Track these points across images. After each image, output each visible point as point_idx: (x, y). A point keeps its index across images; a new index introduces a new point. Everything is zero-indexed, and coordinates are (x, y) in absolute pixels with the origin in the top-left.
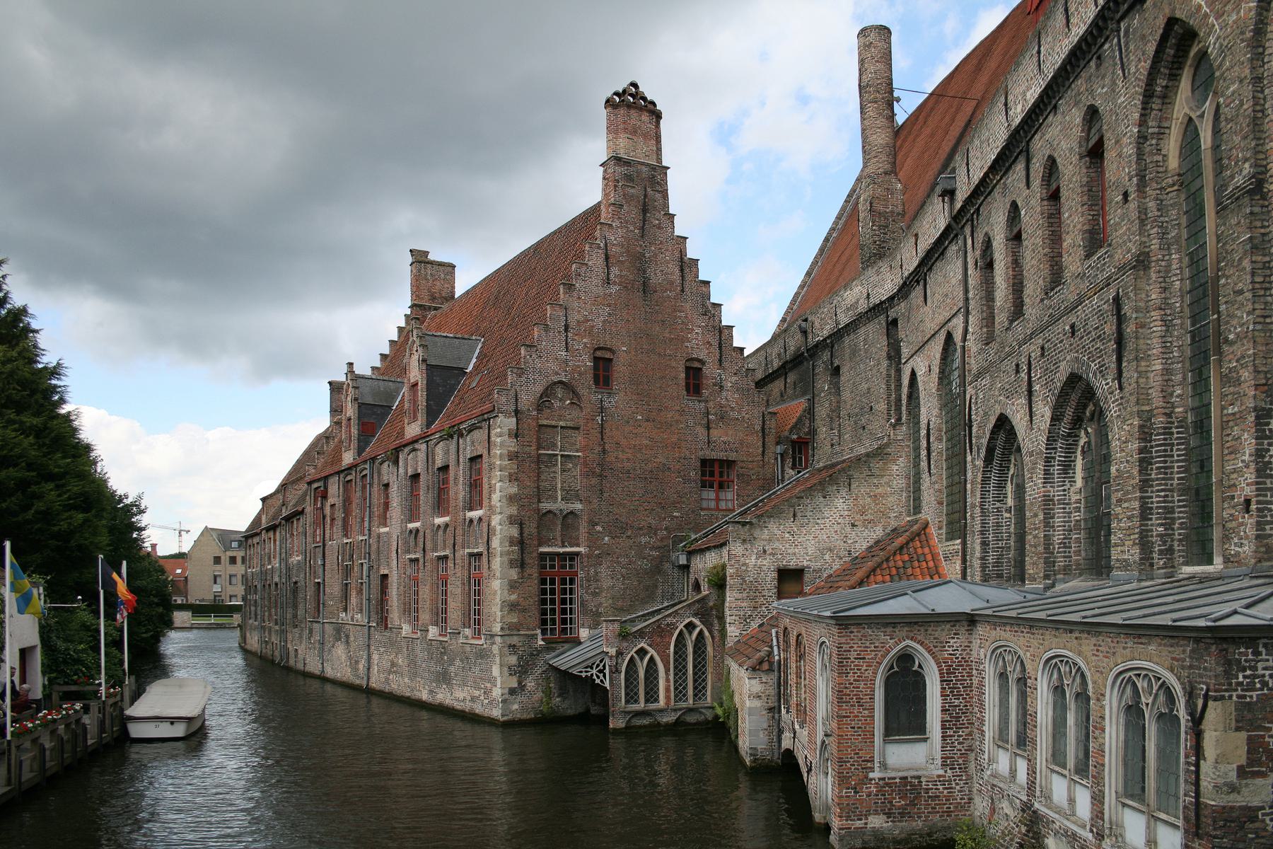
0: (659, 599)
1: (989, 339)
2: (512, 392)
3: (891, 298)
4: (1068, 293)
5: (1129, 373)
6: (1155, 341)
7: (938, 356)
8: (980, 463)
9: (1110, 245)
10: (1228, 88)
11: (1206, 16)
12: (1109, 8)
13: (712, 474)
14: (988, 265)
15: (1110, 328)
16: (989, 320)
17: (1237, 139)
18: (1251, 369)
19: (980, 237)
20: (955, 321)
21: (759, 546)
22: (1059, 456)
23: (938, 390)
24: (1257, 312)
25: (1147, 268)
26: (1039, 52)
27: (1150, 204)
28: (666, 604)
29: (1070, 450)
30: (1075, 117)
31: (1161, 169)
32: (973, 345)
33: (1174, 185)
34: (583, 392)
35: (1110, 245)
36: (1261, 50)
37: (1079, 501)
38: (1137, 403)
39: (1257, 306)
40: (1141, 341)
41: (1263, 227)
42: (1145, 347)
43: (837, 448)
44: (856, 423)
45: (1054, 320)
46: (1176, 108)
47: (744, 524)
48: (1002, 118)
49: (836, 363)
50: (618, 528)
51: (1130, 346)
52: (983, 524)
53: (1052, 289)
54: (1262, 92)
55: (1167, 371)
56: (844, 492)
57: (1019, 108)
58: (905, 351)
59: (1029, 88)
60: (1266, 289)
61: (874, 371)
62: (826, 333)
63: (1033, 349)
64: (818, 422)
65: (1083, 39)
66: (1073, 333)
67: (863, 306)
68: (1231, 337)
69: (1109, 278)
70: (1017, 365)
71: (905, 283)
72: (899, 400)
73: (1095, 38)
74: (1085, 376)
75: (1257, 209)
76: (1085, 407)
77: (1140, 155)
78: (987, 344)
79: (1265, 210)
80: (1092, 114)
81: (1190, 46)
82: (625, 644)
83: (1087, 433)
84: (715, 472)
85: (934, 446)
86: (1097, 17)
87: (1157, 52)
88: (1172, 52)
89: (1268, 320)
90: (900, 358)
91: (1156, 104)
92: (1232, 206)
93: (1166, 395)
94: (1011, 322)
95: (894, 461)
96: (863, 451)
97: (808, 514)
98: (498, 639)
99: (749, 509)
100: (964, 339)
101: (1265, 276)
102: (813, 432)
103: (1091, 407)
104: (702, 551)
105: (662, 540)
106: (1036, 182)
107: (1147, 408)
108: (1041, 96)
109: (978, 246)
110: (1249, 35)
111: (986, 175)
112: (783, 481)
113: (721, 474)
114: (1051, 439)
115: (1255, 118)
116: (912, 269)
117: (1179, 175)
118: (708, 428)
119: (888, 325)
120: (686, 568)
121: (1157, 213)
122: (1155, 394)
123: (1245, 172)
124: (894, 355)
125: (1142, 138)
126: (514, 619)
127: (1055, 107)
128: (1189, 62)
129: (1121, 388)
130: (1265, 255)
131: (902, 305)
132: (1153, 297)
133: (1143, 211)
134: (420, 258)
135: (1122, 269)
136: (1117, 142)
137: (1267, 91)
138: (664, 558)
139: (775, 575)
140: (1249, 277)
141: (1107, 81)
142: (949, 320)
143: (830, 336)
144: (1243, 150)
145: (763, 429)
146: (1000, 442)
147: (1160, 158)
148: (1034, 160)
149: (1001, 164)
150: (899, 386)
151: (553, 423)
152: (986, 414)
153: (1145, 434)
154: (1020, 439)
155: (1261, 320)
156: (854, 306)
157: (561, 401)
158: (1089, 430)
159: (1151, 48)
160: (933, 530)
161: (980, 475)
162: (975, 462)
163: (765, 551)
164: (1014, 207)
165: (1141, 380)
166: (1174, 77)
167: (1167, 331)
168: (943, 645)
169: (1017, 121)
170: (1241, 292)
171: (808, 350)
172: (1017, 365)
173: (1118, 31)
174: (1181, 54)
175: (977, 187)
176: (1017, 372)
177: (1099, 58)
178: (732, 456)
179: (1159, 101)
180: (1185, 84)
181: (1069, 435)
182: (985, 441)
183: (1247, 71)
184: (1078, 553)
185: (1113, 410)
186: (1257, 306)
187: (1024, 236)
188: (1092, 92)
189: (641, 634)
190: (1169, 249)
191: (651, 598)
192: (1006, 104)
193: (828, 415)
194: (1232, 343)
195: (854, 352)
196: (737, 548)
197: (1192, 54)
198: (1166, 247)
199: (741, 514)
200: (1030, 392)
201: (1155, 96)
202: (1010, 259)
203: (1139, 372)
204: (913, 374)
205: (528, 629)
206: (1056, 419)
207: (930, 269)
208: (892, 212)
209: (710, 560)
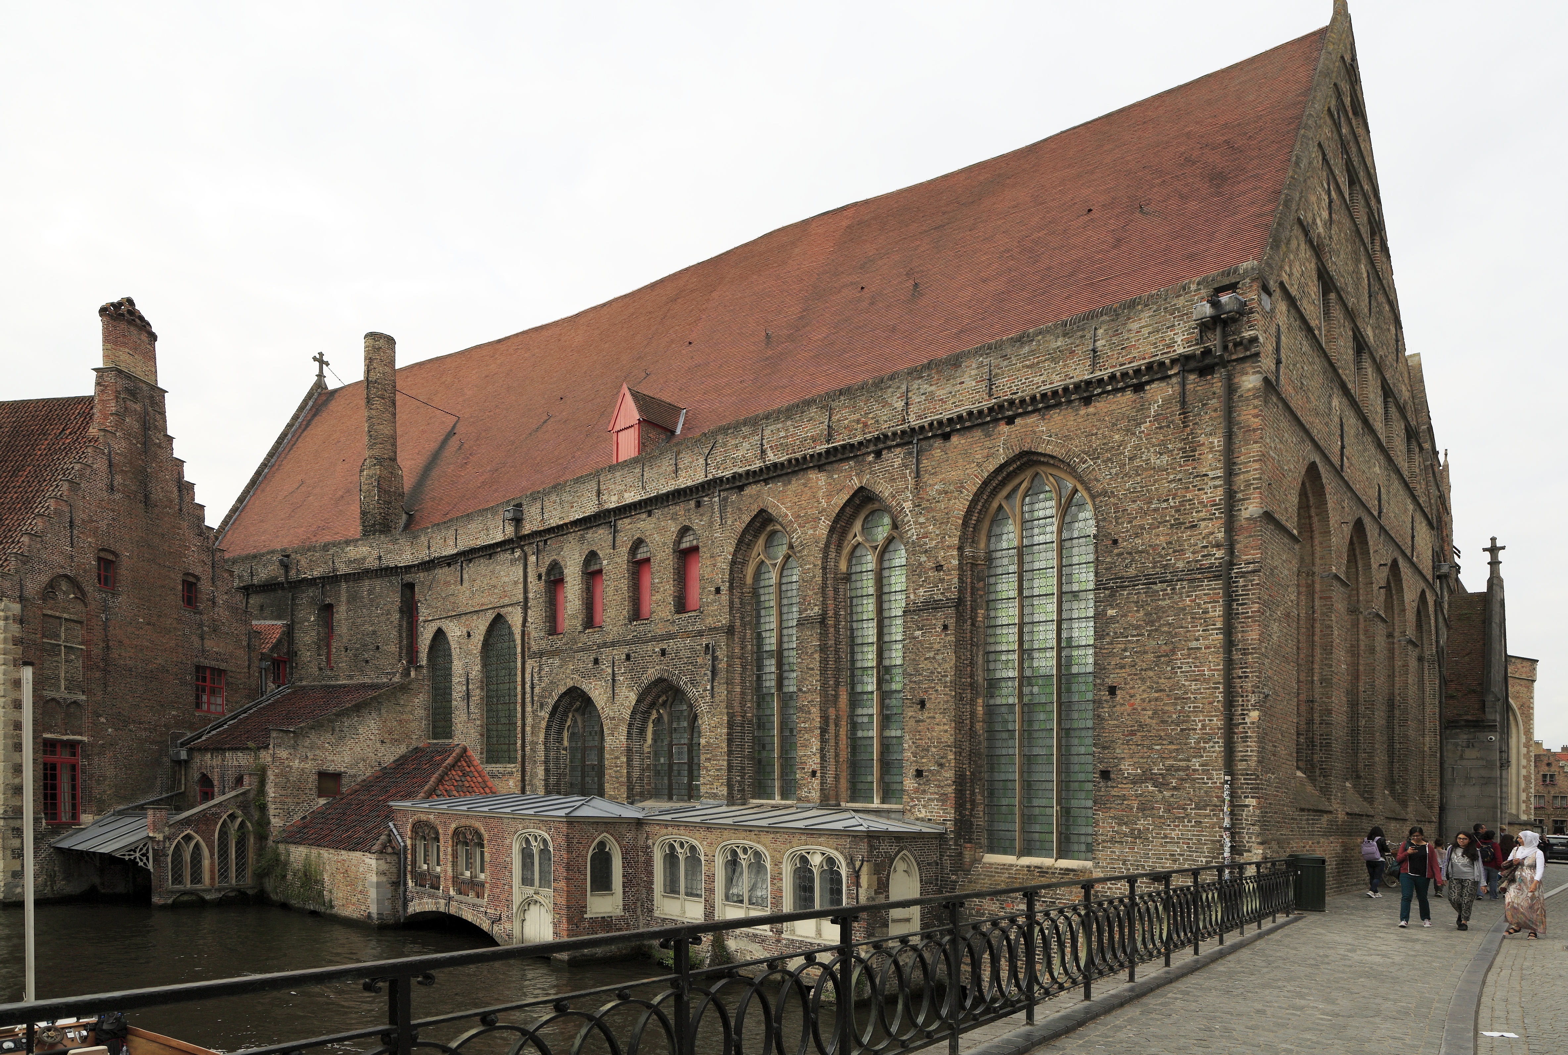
2: (17, 578)
13: (204, 679)
34: (89, 589)
37: (649, 753)
52: (546, 756)
84: (207, 678)
118: (202, 639)
151: (57, 614)
157: (65, 594)
160: (476, 757)
184: (649, 784)
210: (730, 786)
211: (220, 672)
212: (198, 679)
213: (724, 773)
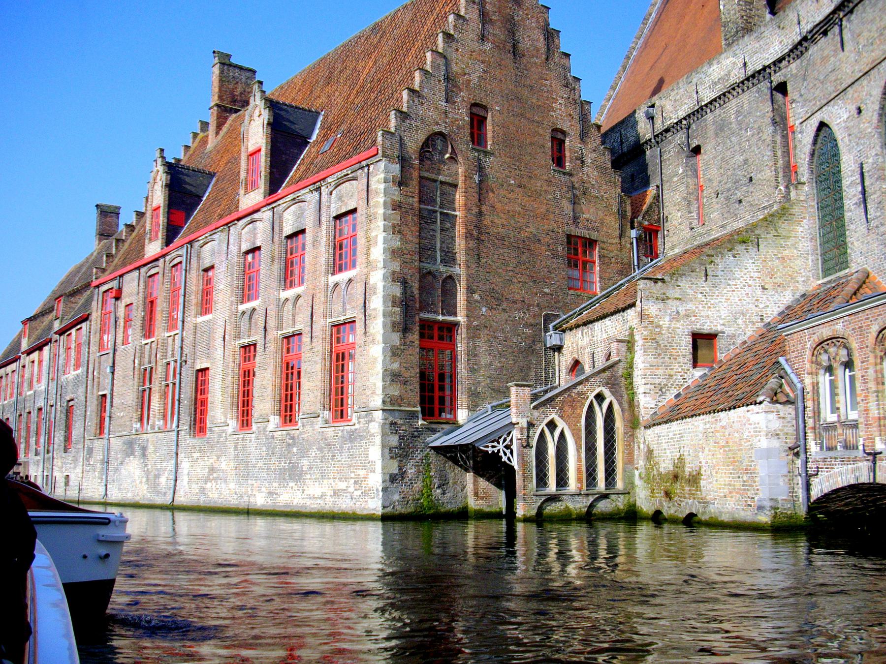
3: (780, 60)
23: (877, 127)
44: (727, 199)
49: (694, 143)
50: (495, 299)
62: (682, 114)
67: (737, 75)
82: (536, 413)
95: (799, 223)
96: (741, 224)
97: (720, 273)
98: (379, 415)
99: (611, 292)
119: (772, 90)
124: (780, 121)
126: (395, 391)
134: (225, 62)
138: (536, 338)
139: (689, 339)
143: (689, 116)
163: (678, 312)
171: (655, 136)
178: (594, 236)
193: (685, 199)
195: (721, 127)
196: (652, 309)
205: (409, 405)
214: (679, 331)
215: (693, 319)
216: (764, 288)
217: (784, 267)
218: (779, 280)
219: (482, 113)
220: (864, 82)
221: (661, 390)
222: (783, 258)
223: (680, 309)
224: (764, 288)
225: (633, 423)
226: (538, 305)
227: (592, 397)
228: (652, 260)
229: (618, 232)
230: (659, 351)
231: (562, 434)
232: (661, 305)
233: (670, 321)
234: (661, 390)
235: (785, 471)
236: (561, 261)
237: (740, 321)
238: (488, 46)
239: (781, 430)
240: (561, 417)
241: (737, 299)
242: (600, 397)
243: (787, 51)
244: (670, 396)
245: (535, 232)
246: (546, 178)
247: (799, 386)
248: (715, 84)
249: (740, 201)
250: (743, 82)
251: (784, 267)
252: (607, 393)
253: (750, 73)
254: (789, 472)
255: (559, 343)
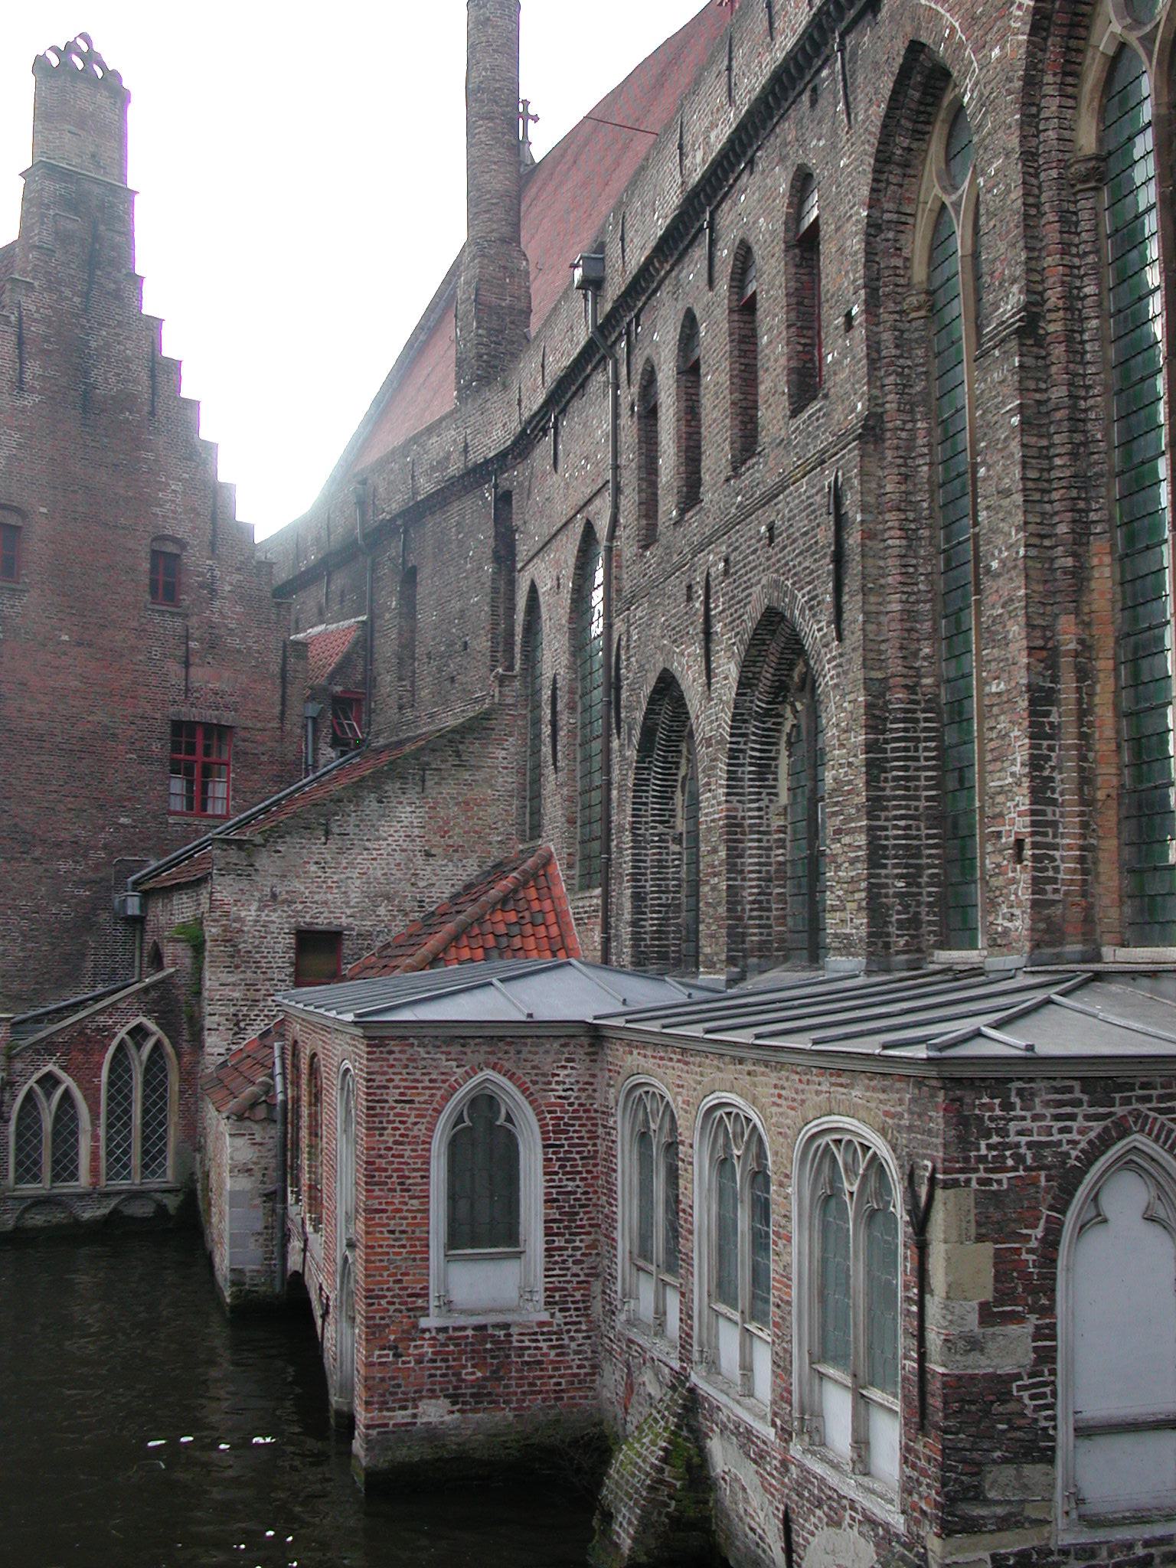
0: (87, 980)
1: (649, 538)
3: (502, 456)
4: (763, 472)
5: (854, 613)
6: (890, 562)
7: (572, 561)
8: (632, 754)
9: (826, 396)
10: (990, 164)
11: (961, 43)
12: (828, 13)
13: (191, 750)
14: (649, 414)
15: (825, 535)
16: (649, 506)
17: (1002, 246)
18: (1022, 620)
19: (639, 365)
20: (597, 502)
21: (266, 882)
22: (752, 749)
23: (571, 620)
24: (1031, 528)
25: (879, 440)
26: (729, 69)
27: (885, 336)
28: (100, 989)
29: (768, 739)
30: (782, 183)
31: (902, 281)
32: (627, 547)
33: (918, 309)
35: (826, 396)
36: (1034, 110)
38: (864, 666)
39: (1031, 518)
40: (870, 562)
41: (1037, 390)
42: (875, 572)
43: (409, 714)
44: (440, 671)
45: (746, 514)
46: (924, 187)
47: (240, 844)
48: (672, 165)
49: (412, 560)
51: (854, 567)
53: (743, 462)
54: (1036, 176)
55: (909, 615)
56: (412, 794)
57: (699, 155)
58: (523, 550)
59: (713, 125)
60: (1044, 491)
61: (472, 581)
63: (713, 561)
64: (380, 666)
65: (791, 57)
66: (771, 539)
68: (995, 564)
69: (824, 451)
70: (689, 587)
71: (524, 430)
72: (510, 634)
73: (809, 60)
74: (788, 614)
75: (1030, 361)
76: (791, 666)
77: (870, 253)
78: (646, 547)
79: (1041, 363)
80: (803, 182)
81: (943, 90)
83: (795, 711)
84: (195, 747)
85: (564, 718)
86: (810, 24)
87: (895, 92)
88: (917, 95)
89: (1047, 543)
90: (514, 562)
91: (894, 175)
92: (997, 353)
93: (909, 655)
94: (682, 512)
95: (499, 742)
97: (350, 829)
99: (254, 816)
100: (612, 536)
101: (1042, 470)
102: (370, 681)
103: (800, 668)
104: (167, 891)
105: (97, 868)
106: (723, 286)
107: (879, 675)
108: (730, 140)
109: (637, 378)
110: (1018, 84)
111: (649, 260)
112: (315, 768)
113: (207, 754)
114: (738, 718)
115: (1027, 216)
116: (535, 408)
117: (930, 293)
120: (137, 923)
121: (894, 352)
122: (891, 651)
123: (1013, 300)
125: (873, 228)
127: (751, 163)
128: (942, 115)
129: (840, 638)
130: (1041, 436)
131: (520, 467)
132: (889, 488)
133: (873, 345)
135: (841, 440)
136: (837, 229)
137: (1043, 176)
139: (291, 940)
140: (1017, 473)
141: (825, 128)
142: (589, 501)
143: (402, 514)
144: (1009, 265)
145: (284, 670)
146: (663, 718)
147: (899, 262)
148: (720, 244)
149: (674, 243)
150: (511, 609)
152: (641, 666)
153: (875, 718)
154: (693, 716)
155: (1035, 541)
156: (443, 463)
158: (799, 706)
159: (887, 84)
161: (631, 775)
162: (625, 750)
163: (274, 896)
164: (690, 322)
165: (871, 627)
166: (920, 135)
167: (909, 547)
168: (546, 1079)
169: (696, 177)
170: (1006, 493)
171: (365, 536)
172: (689, 587)
173: (842, 50)
174: (929, 100)
175: (636, 280)
176: (689, 599)
177: (814, 90)
178: (228, 718)
179: (898, 171)
180: (936, 147)
181: (767, 713)
182: (639, 716)
183: (1014, 142)
185: (828, 677)
186: (1031, 518)
187: (703, 370)
188: (802, 143)
189: (47, 1048)
190: (912, 412)
191: (71, 976)
192: (680, 147)
194: (997, 575)
197: (945, 103)
198: (908, 408)
199: (244, 824)
200: (708, 634)
201: (892, 164)
202: (683, 404)
203: (865, 613)
204: (533, 589)
206: (745, 683)
207: (563, 411)
208: (511, 307)
209: (182, 909)
210: (875, 909)
211: (219, 732)
212: (176, 748)
213: (861, 869)
214: (273, 928)
215: (300, 907)
216: (428, 854)
217: (468, 818)
218: (457, 840)
219: (14, 520)
220: (562, 538)
221: (238, 1024)
222: (467, 803)
223: (278, 890)
224: (428, 855)
225: (189, 1077)
226: (105, 847)
227: (122, 1033)
228: (343, 753)
229: (277, 710)
230: (237, 960)
231: (67, 1095)
232: (244, 884)
233: (259, 909)
234: (237, 1024)
235: (259, 1226)
236: (156, 767)
237: (382, 911)
238: (30, 400)
239: (255, 1163)
240: (64, 1068)
241: (379, 873)
242: (139, 1033)
243: (509, 443)
244: (252, 1035)
245: (106, 721)
246: (135, 624)
247: (280, 1097)
248: (433, 469)
249: (452, 680)
250: (462, 477)
251: (468, 818)
252: (152, 1026)
253: (470, 465)
254: (266, 1228)
255: (137, 912)
